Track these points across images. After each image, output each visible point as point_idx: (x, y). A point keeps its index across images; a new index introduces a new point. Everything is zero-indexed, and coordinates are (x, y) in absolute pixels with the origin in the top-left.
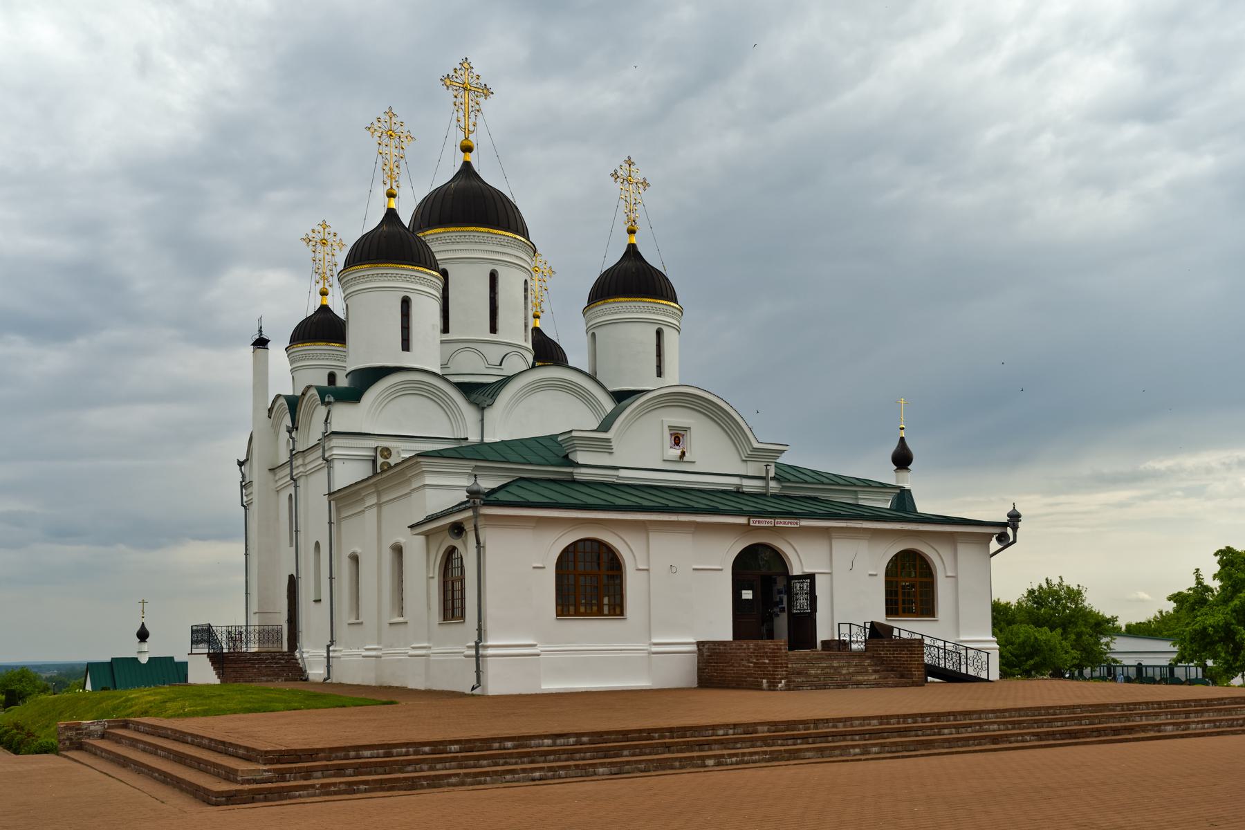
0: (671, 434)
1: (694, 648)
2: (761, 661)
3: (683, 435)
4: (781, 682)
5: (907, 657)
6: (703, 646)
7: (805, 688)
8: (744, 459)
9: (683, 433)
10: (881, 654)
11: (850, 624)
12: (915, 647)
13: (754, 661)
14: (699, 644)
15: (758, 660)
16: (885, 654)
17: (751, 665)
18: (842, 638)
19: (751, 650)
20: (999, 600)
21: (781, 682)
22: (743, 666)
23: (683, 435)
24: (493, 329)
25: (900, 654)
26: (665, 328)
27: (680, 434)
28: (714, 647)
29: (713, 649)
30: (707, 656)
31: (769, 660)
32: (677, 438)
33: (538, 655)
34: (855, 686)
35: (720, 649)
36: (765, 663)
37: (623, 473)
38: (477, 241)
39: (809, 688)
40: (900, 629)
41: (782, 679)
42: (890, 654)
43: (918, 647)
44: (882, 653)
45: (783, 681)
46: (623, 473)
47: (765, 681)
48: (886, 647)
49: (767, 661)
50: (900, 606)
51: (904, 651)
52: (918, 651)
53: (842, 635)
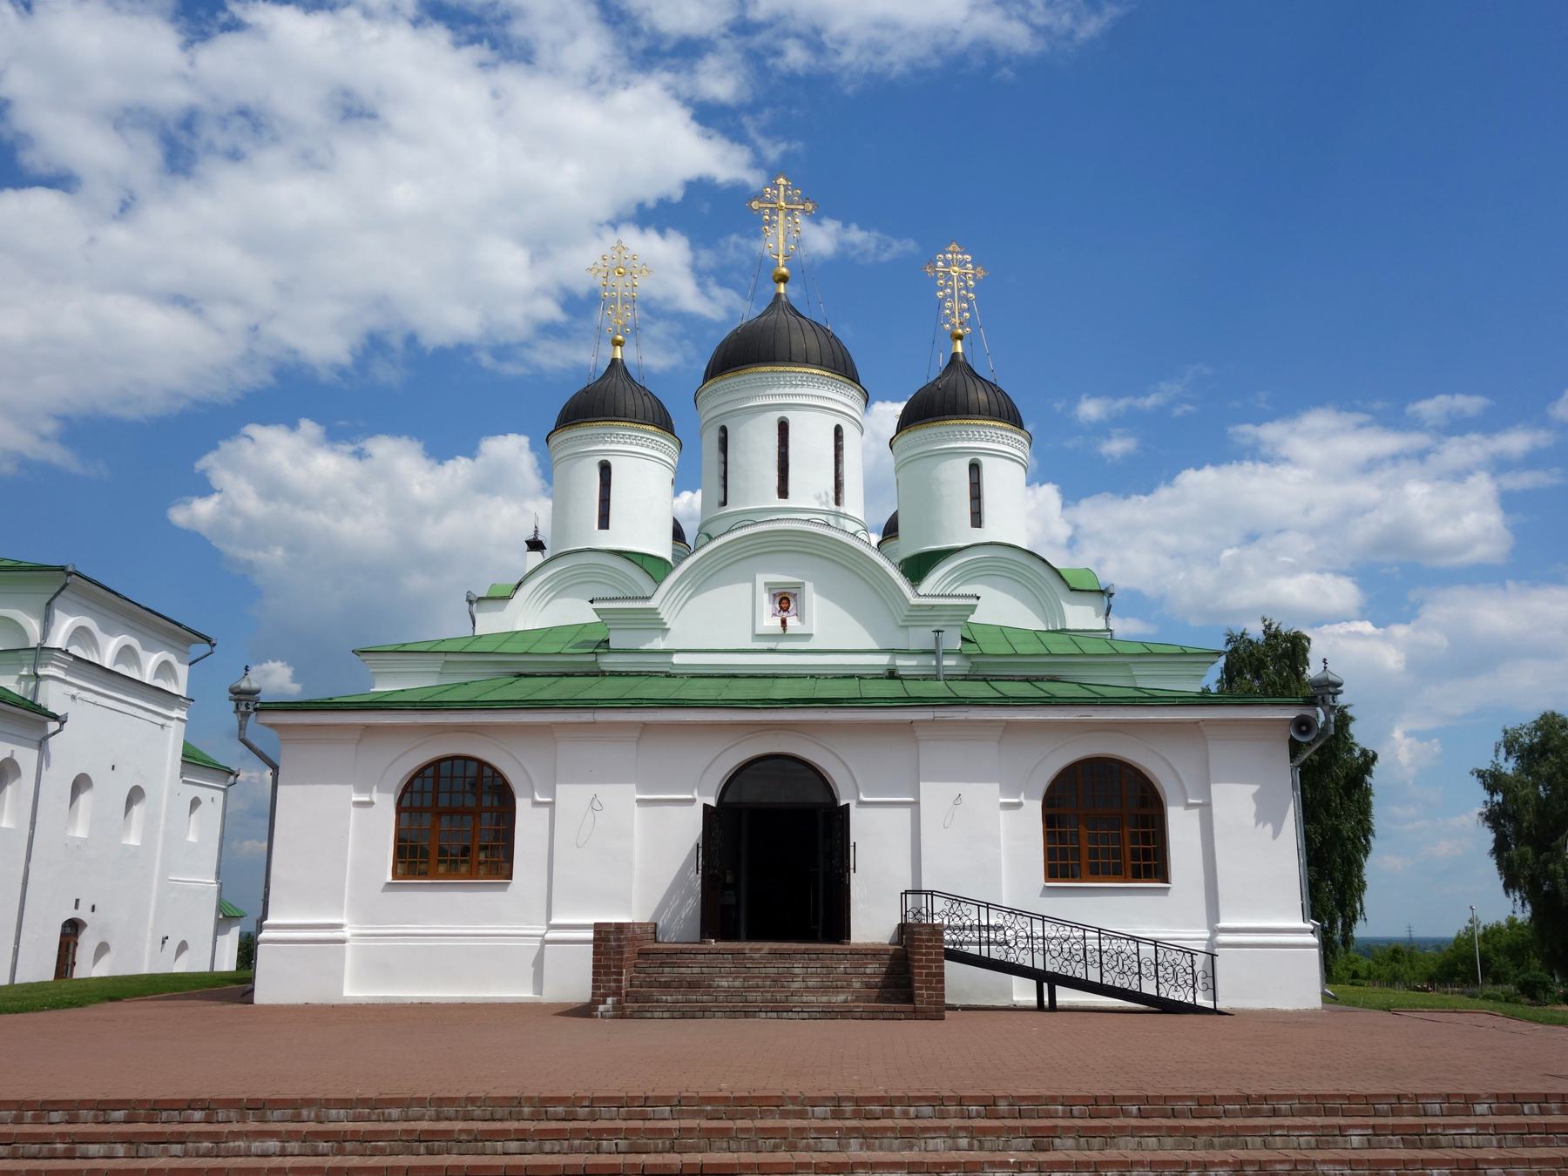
0: (774, 595)
1: (590, 935)
3: (795, 595)
4: (604, 1002)
7: (656, 1015)
8: (901, 623)
9: (793, 591)
12: (921, 940)
14: (598, 928)
21: (604, 1002)
23: (795, 595)
24: (783, 492)
26: (981, 458)
27: (789, 593)
32: (785, 600)
33: (343, 941)
34: (775, 1015)
37: (677, 659)
38: (759, 384)
39: (666, 1015)
41: (608, 995)
46: (677, 659)
50: (1085, 859)
52: (927, 947)
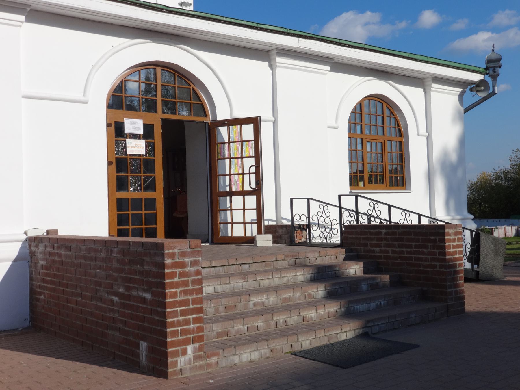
2: (135, 293)
4: (184, 352)
5: (433, 260)
6: (37, 246)
10: (374, 251)
11: (308, 199)
13: (121, 290)
15: (127, 289)
16: (381, 251)
17: (116, 299)
18: (296, 223)
19: (115, 265)
20: (494, 169)
22: (100, 299)
25: (418, 253)
28: (51, 250)
29: (50, 254)
30: (42, 267)
31: (153, 294)
35: (60, 255)
36: (144, 301)
40: (390, 206)
41: (187, 342)
42: (394, 252)
43: (454, 240)
44: (378, 249)
45: (190, 349)
47: (144, 345)
48: (386, 239)
49: (148, 296)
51: (426, 247)
53: (296, 218)
